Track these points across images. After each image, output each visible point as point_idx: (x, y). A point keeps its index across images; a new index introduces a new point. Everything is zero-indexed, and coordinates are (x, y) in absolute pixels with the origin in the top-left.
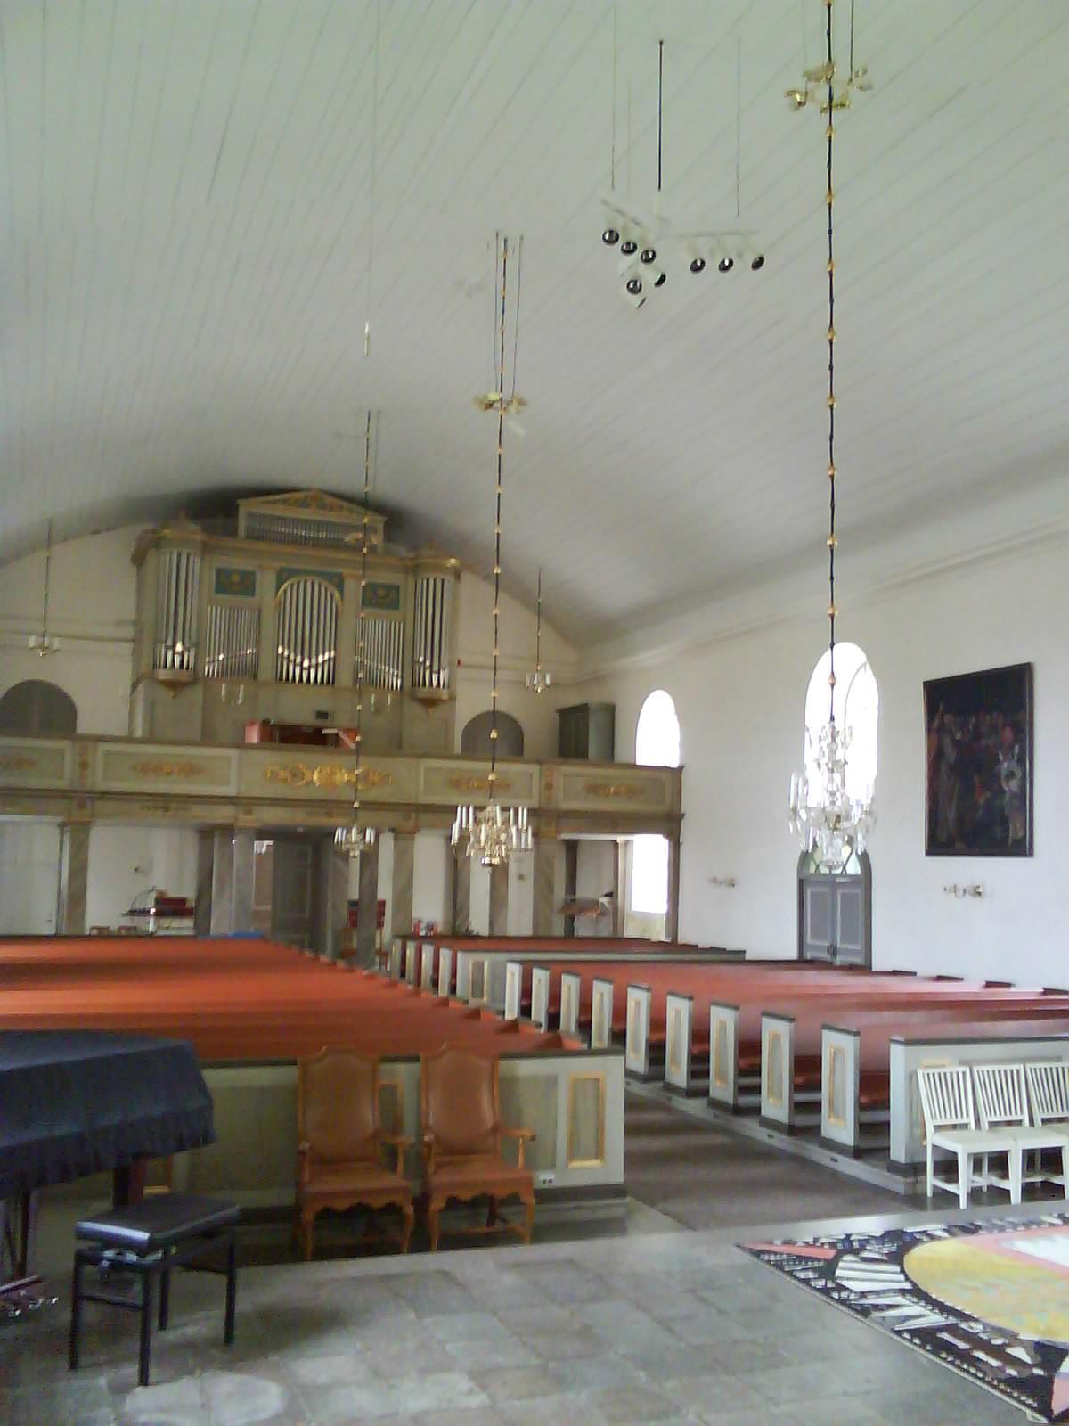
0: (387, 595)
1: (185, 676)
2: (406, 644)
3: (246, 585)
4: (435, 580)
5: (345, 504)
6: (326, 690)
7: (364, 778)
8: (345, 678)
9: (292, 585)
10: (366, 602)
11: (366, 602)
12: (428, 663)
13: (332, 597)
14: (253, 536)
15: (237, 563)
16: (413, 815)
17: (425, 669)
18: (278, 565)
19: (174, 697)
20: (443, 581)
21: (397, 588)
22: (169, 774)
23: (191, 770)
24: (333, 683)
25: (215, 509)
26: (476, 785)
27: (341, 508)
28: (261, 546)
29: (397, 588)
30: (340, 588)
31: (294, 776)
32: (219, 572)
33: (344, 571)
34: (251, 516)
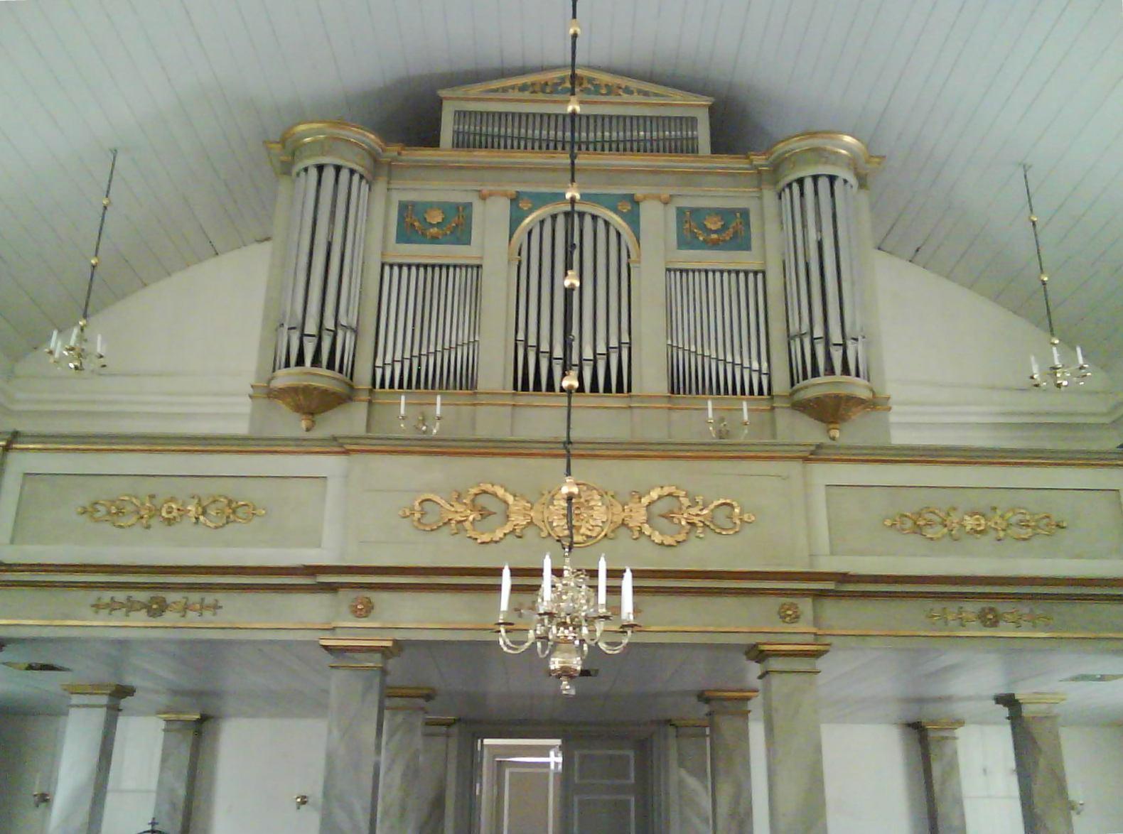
0: (725, 227)
1: (324, 379)
2: (769, 302)
3: (458, 225)
4: (815, 178)
5: (633, 84)
6: (613, 400)
7: (663, 514)
8: (650, 376)
9: (542, 222)
10: (686, 241)
11: (686, 241)
12: (818, 332)
13: (619, 234)
14: (461, 142)
15: (435, 191)
16: (806, 605)
17: (813, 340)
18: (513, 189)
19: (308, 430)
20: (832, 179)
21: (745, 213)
22: (170, 522)
23: (233, 511)
24: (629, 390)
25: (410, 118)
26: (970, 522)
27: (628, 91)
28: (481, 156)
29: (745, 213)
30: (633, 220)
31: (484, 514)
32: (404, 208)
33: (639, 192)
34: (461, 115)
